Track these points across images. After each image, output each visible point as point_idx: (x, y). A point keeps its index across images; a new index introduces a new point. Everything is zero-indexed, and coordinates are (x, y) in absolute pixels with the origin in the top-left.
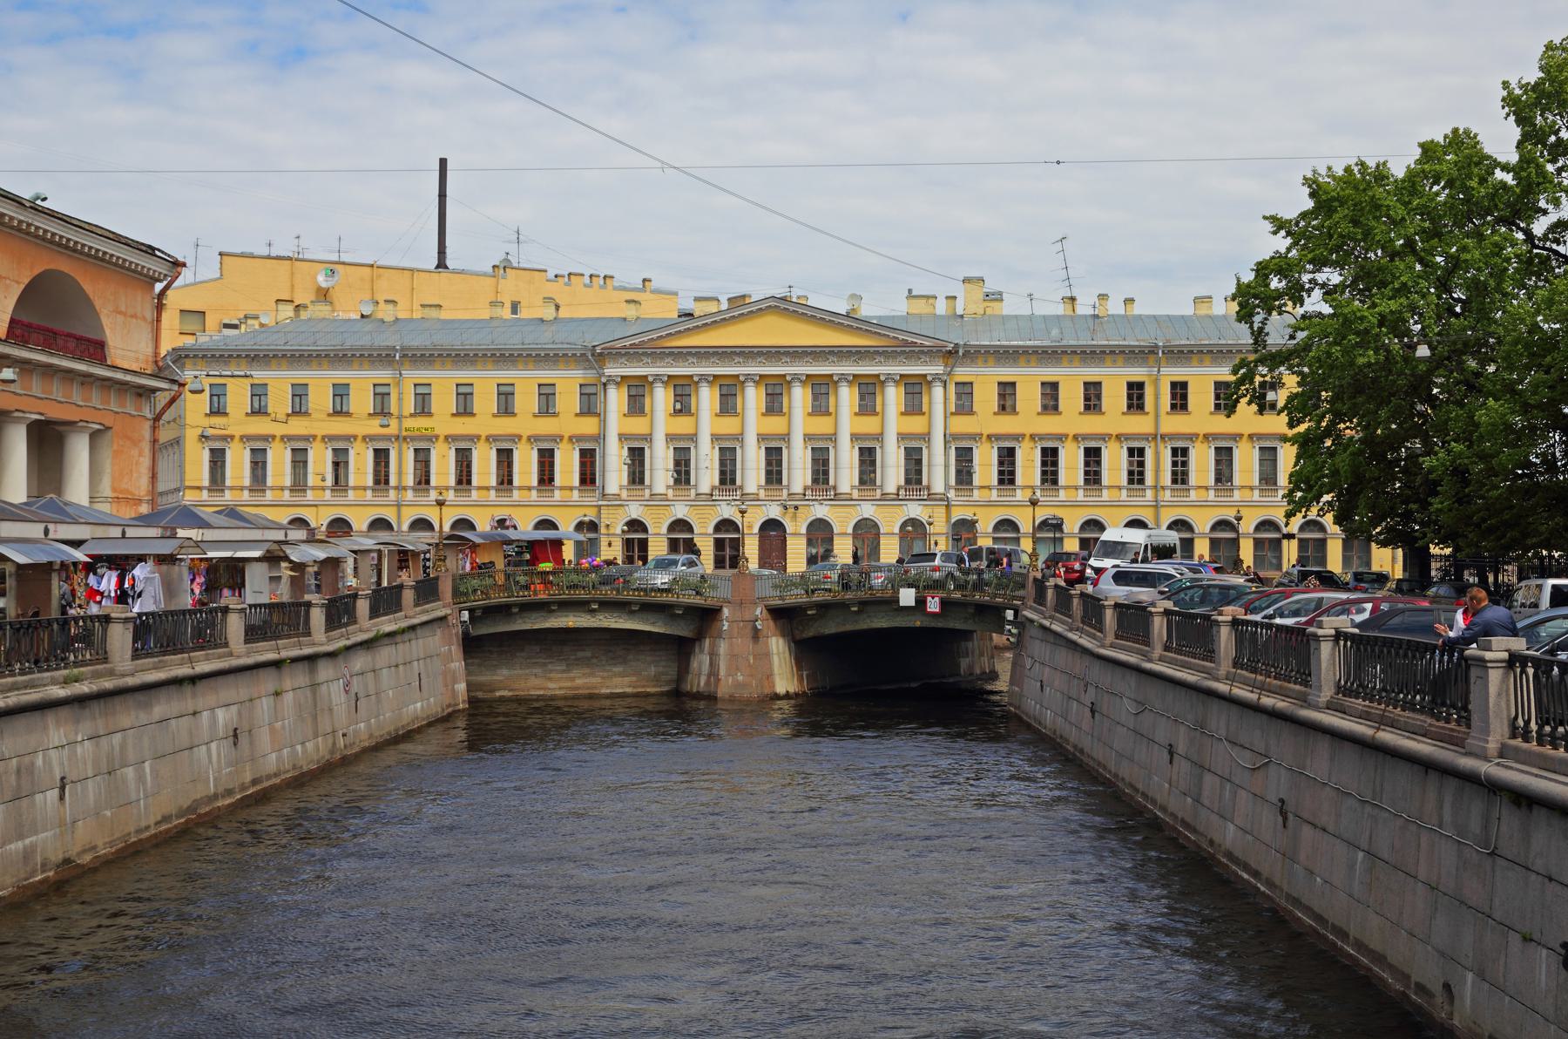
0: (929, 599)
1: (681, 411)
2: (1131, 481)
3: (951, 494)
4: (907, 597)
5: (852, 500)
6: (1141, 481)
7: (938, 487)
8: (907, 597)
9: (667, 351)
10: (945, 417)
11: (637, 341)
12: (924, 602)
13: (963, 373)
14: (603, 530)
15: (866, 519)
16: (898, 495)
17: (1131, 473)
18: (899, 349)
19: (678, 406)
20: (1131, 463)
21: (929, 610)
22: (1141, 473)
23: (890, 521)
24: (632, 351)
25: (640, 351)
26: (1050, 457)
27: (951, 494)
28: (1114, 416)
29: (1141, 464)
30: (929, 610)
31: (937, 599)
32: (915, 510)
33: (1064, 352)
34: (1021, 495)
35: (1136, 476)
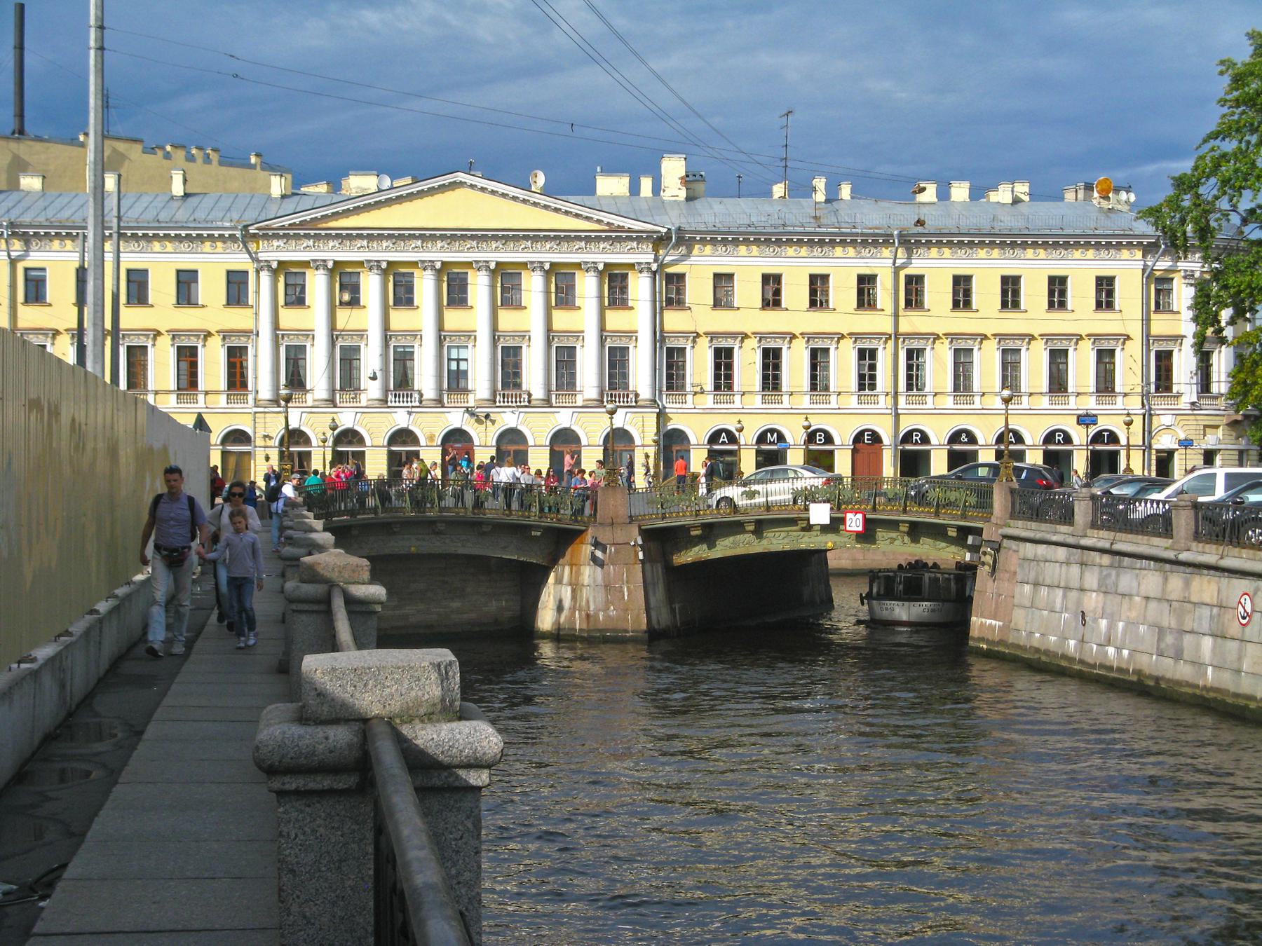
0: (849, 516)
2: (861, 387)
4: (820, 514)
6: (873, 387)
8: (820, 514)
9: (333, 232)
11: (297, 221)
12: (843, 521)
14: (259, 442)
17: (861, 377)
18: (603, 234)
20: (860, 366)
21: (848, 528)
22: (873, 377)
24: (291, 232)
25: (302, 232)
26: (771, 359)
29: (873, 367)
30: (848, 528)
31: (860, 516)
34: (1074, 404)
35: (866, 381)
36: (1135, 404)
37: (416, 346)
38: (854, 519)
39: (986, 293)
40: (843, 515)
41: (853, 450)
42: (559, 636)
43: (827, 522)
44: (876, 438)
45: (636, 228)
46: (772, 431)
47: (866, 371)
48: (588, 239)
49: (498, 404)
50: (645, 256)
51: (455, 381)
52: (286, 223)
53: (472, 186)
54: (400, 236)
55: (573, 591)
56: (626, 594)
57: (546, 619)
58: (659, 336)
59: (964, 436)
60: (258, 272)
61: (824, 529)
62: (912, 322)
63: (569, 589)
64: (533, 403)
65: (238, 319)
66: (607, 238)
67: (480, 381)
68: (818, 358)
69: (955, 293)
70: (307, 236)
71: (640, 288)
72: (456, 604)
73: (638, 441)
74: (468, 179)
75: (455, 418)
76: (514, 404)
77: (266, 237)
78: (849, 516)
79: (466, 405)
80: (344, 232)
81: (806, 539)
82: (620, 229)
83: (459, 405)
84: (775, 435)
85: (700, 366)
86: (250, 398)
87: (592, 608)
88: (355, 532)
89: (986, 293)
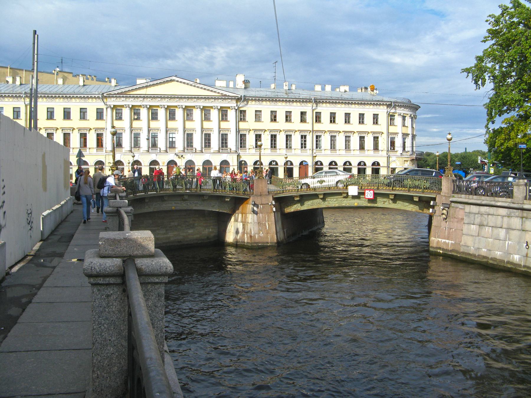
0: (367, 191)
1: (137, 119)
4: (353, 190)
6: (305, 147)
9: (132, 96)
11: (120, 92)
12: (364, 194)
16: (219, 151)
17: (302, 144)
18: (220, 97)
19: (136, 117)
20: (302, 141)
21: (366, 197)
22: (305, 144)
23: (216, 161)
24: (118, 96)
25: (121, 96)
28: (296, 124)
29: (305, 141)
30: (366, 197)
31: (372, 192)
35: (303, 145)
36: (385, 153)
37: (159, 133)
38: (369, 193)
39: (340, 118)
40: (364, 191)
42: (236, 245)
43: (356, 194)
45: (231, 95)
46: (274, 161)
47: (303, 142)
48: (215, 99)
50: (233, 104)
51: (172, 145)
52: (116, 93)
53: (177, 81)
54: (154, 97)
55: (243, 225)
56: (267, 226)
57: (230, 237)
58: (238, 130)
60: (107, 109)
61: (354, 197)
62: (317, 127)
63: (241, 224)
64: (197, 152)
65: (100, 124)
66: (221, 98)
67: (180, 144)
68: (288, 138)
69: (331, 118)
70: (123, 97)
71: (232, 115)
72: (190, 231)
73: (231, 164)
74: (176, 79)
75: (171, 156)
77: (109, 97)
78: (367, 191)
80: (135, 96)
81: (345, 202)
82: (225, 95)
85: (250, 140)
86: (104, 150)
87: (252, 233)
88: (147, 201)
89: (340, 118)
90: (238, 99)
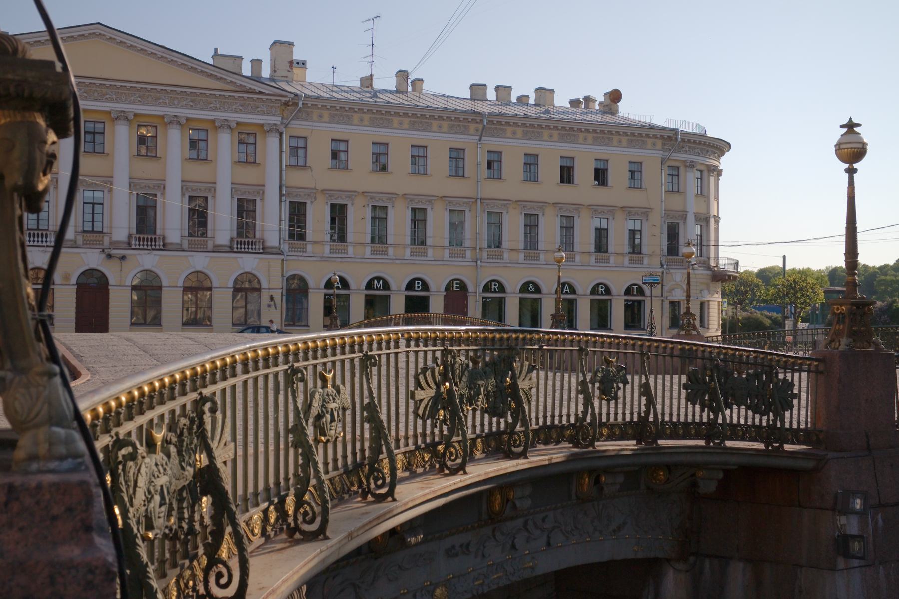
3: (285, 247)
5: (183, 250)
7: (272, 240)
10: (281, 170)
13: (299, 127)
15: (247, 273)
27: (285, 247)
32: (249, 262)
33: (397, 114)
41: (445, 296)
44: (463, 286)
46: (378, 278)
49: (133, 247)
59: (531, 286)
62: (492, 189)
64: (169, 247)
73: (264, 284)
76: (150, 247)
79: (101, 246)
83: (98, 246)
84: (381, 281)
90: (286, 104)
